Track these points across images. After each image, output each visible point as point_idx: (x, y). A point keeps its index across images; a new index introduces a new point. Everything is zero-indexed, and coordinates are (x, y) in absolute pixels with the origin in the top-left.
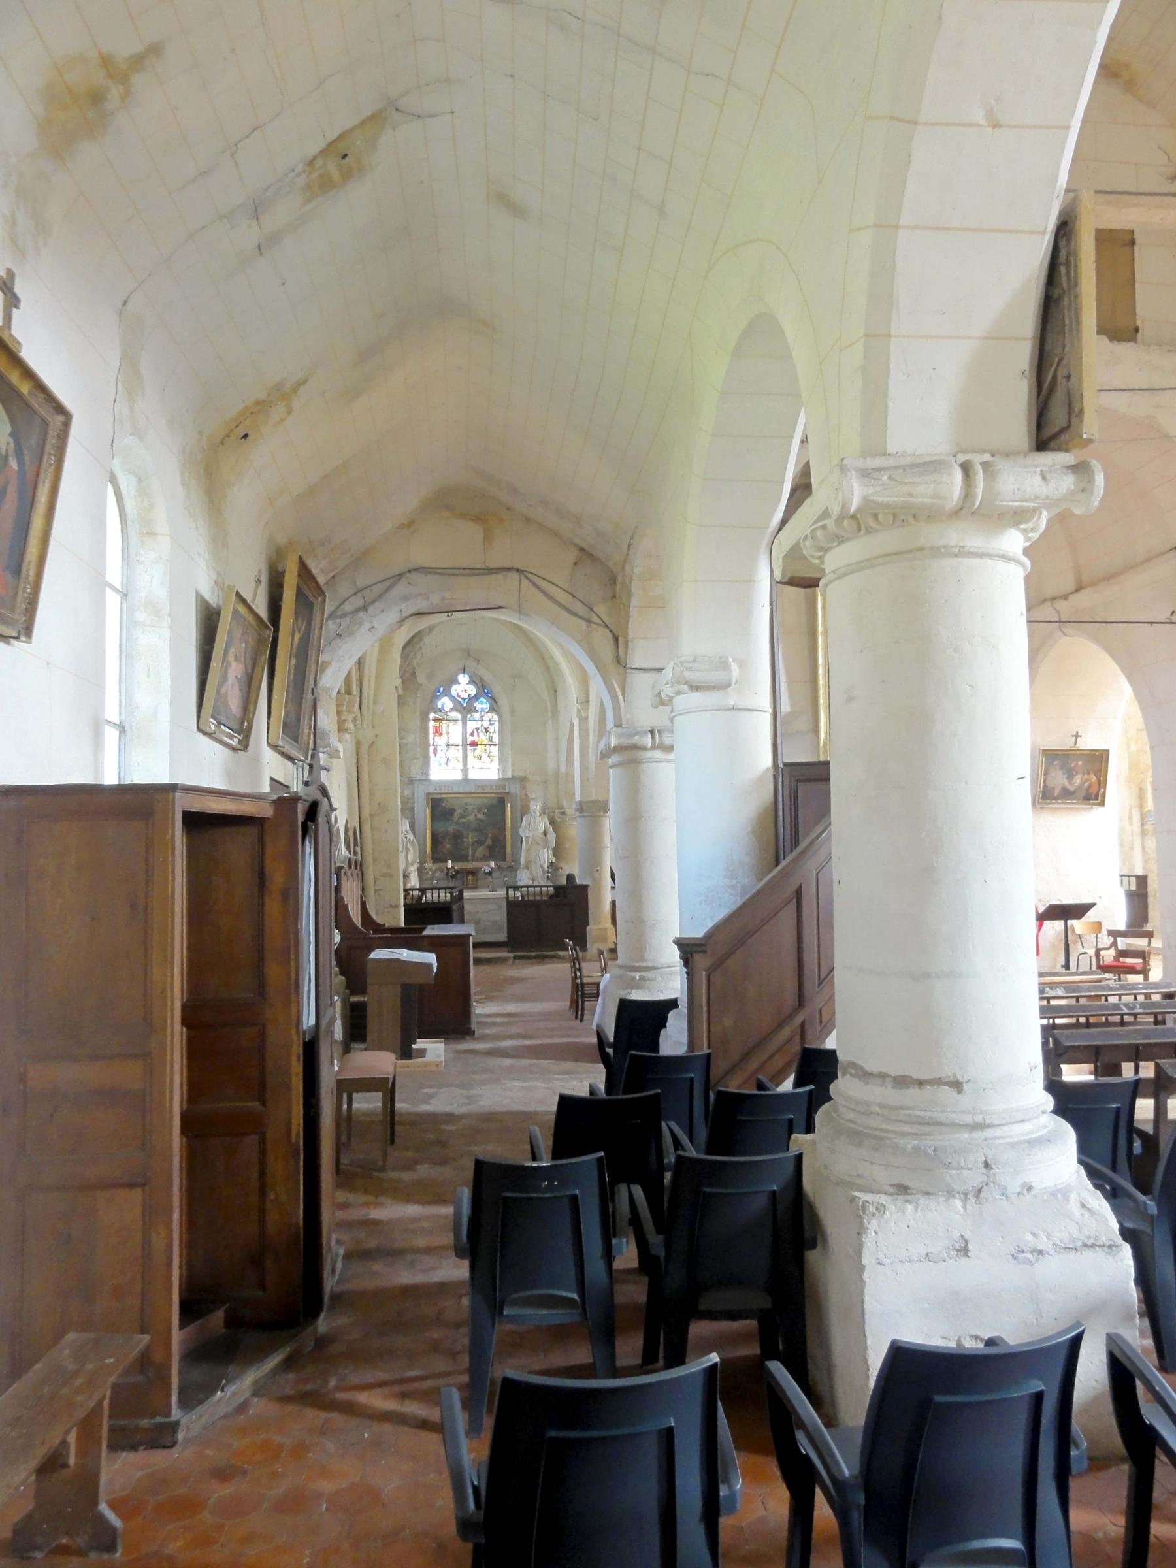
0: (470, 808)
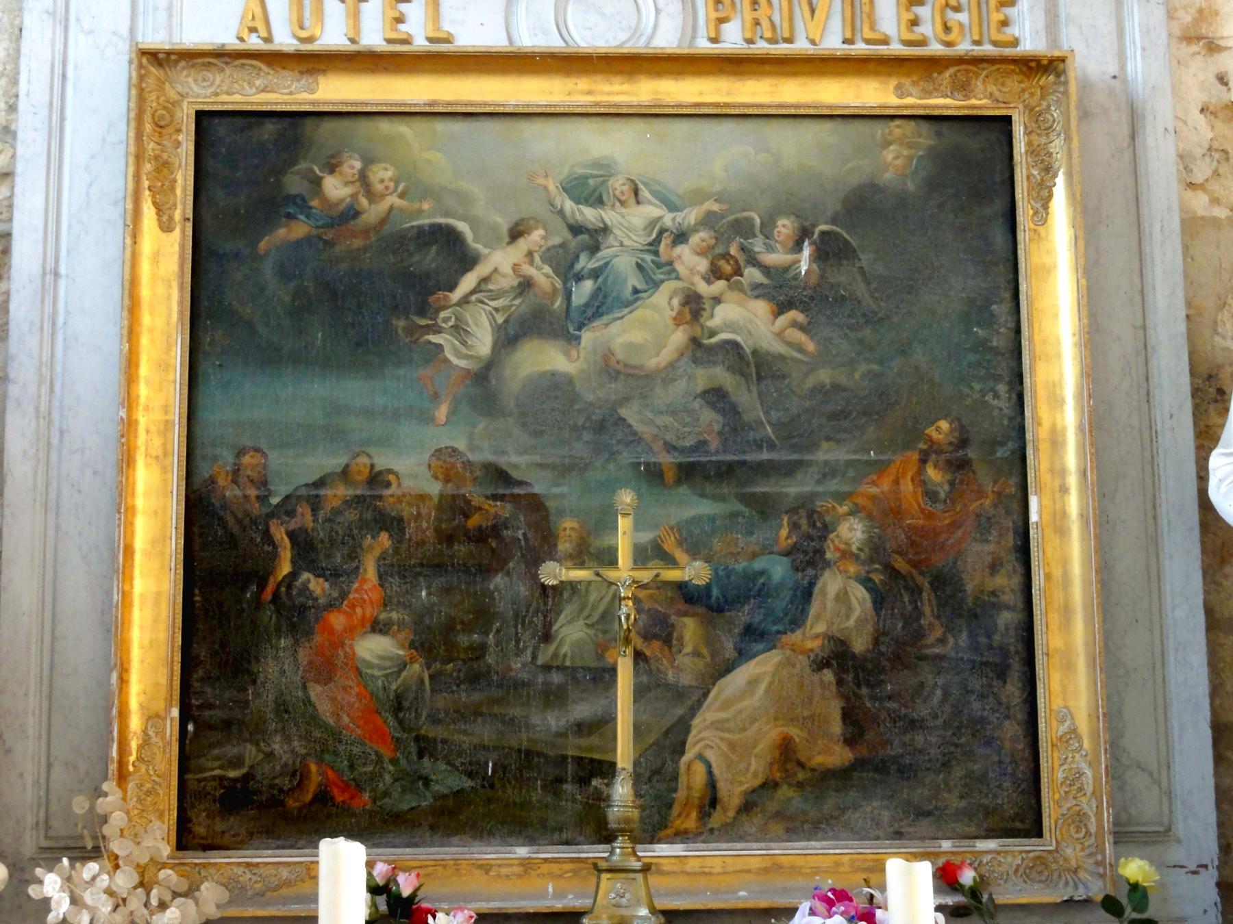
0: (629, 224)
